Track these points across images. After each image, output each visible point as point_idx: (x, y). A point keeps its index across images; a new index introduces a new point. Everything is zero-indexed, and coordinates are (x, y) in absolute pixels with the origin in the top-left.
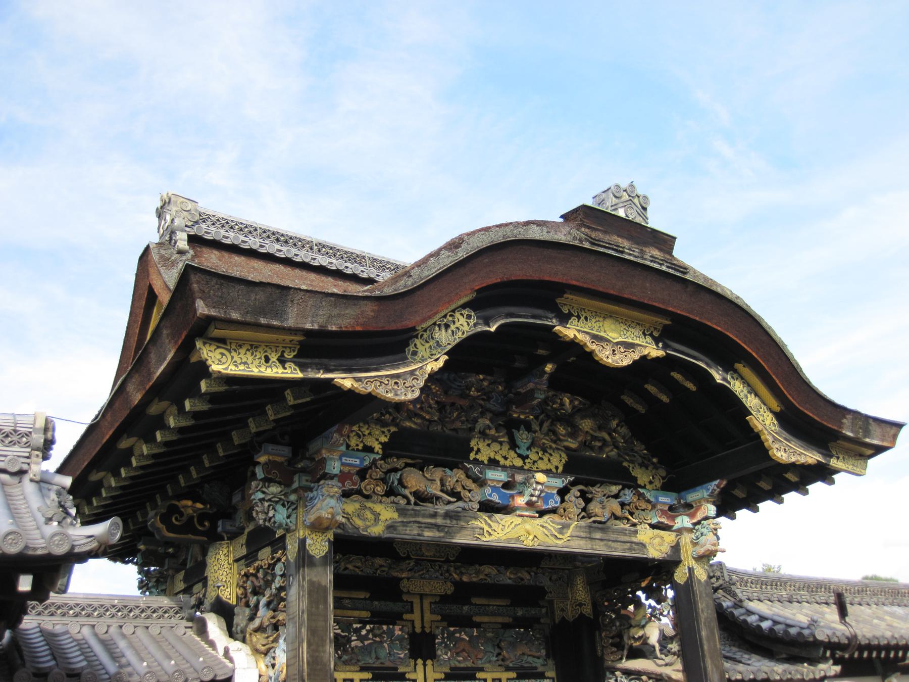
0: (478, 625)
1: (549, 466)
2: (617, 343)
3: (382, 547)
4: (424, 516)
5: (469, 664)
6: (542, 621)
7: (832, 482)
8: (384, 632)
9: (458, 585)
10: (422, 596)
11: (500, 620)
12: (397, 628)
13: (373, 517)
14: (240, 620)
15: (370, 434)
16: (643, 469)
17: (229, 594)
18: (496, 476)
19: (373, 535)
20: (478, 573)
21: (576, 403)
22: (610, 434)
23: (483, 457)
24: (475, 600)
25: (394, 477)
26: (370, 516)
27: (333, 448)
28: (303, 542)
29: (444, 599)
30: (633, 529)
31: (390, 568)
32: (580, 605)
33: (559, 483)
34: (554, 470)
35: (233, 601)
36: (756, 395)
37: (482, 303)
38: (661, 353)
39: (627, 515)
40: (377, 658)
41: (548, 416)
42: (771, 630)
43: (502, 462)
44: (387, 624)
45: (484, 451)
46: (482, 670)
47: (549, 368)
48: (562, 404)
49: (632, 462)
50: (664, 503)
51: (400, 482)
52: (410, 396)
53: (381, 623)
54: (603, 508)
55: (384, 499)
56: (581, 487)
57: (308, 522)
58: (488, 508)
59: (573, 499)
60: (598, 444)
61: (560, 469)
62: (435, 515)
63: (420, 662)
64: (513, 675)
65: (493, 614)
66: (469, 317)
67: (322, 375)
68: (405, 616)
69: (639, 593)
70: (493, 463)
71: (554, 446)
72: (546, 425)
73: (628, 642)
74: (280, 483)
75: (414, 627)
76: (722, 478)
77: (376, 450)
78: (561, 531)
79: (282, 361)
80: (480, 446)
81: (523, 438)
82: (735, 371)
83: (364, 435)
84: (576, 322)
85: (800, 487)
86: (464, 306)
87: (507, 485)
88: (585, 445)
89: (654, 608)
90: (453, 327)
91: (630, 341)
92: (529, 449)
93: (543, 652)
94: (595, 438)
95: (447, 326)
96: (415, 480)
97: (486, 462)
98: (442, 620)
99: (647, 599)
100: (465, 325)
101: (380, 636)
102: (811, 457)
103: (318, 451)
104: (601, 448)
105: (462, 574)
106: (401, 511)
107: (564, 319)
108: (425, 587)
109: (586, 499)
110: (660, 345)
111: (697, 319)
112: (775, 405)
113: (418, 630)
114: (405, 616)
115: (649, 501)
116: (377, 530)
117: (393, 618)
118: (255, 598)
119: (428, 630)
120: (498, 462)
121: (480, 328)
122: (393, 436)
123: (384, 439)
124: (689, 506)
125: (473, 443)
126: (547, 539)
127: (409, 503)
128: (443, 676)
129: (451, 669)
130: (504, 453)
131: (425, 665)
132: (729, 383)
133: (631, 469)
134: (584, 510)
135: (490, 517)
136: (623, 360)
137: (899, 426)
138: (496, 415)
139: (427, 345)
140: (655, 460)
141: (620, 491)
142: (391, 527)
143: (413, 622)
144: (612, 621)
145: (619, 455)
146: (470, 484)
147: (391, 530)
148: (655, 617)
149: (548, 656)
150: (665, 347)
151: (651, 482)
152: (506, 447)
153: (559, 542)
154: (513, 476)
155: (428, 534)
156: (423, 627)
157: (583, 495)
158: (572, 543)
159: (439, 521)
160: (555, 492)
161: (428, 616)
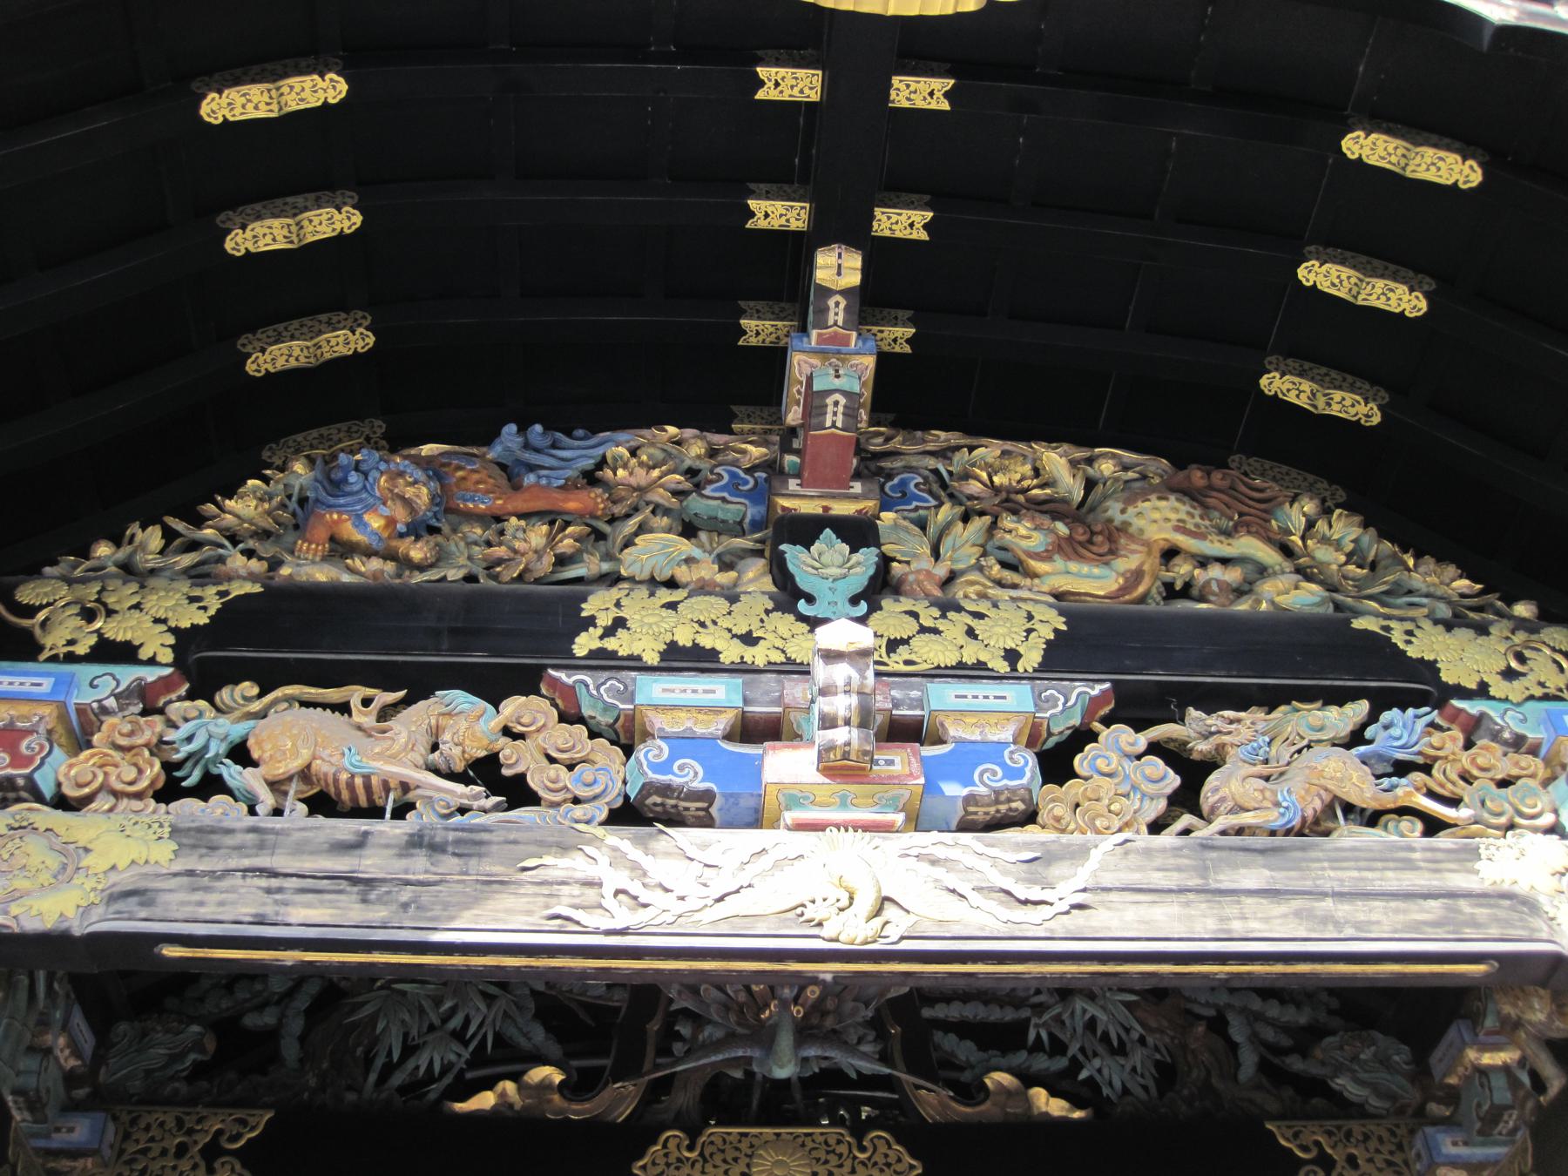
1: (971, 654)
4: (300, 849)
13: (54, 862)
15: (137, 606)
19: (31, 925)
22: (1287, 551)
23: (643, 642)
43: (731, 652)
45: (648, 628)
47: (838, 269)
51: (240, 754)
59: (1114, 761)
61: (1032, 658)
62: (359, 844)
70: (685, 659)
71: (1005, 594)
77: (144, 654)
83: (110, 613)
94: (1203, 562)
96: (299, 733)
97: (652, 658)
115: (1518, 743)
120: (713, 654)
125: (598, 605)
127: (252, 811)
133: (1397, 638)
135: (639, 842)
145: (1338, 607)
147: (131, 904)
151: (1509, 674)
155: (307, 915)
159: (370, 864)
160: (1007, 735)
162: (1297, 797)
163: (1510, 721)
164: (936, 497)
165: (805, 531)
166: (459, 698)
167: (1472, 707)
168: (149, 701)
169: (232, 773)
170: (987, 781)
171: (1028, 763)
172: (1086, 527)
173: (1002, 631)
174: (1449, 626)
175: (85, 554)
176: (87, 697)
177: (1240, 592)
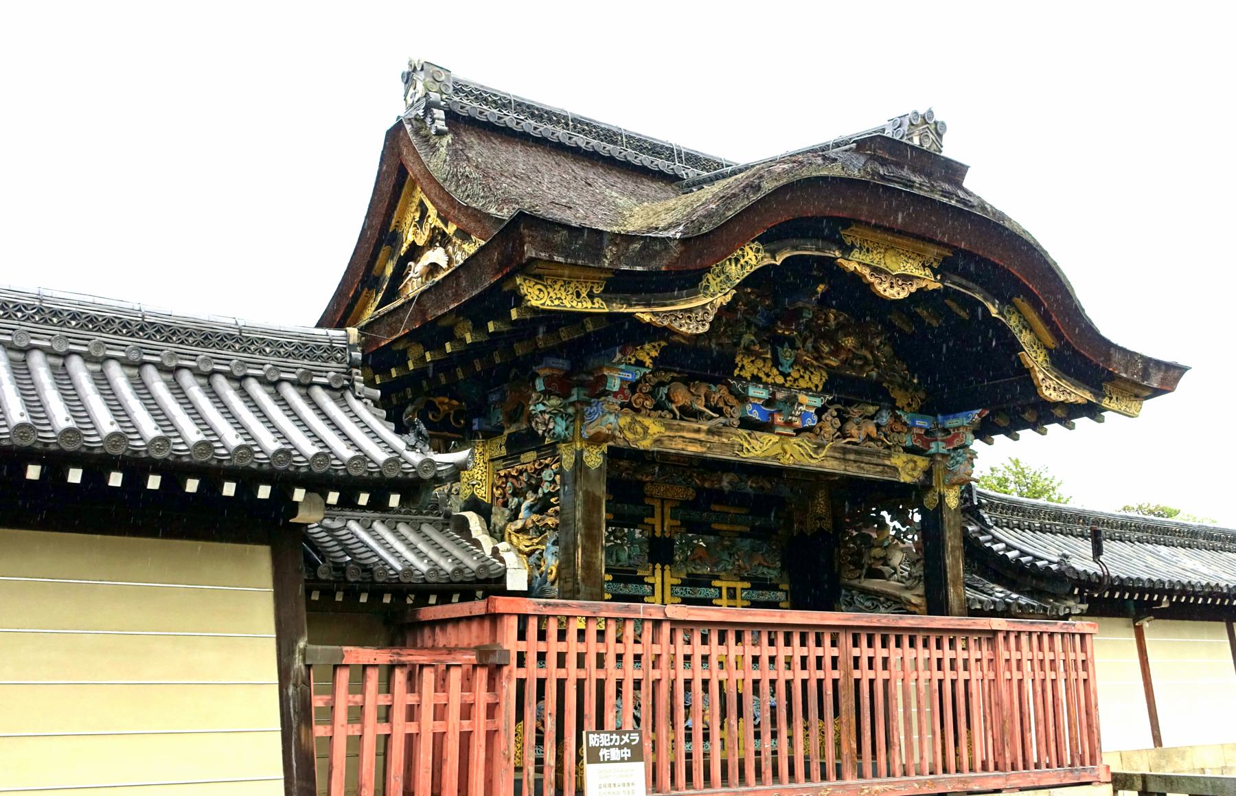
1: (810, 385)
2: (896, 276)
3: (640, 457)
4: (689, 431)
6: (780, 532)
7: (1101, 420)
8: (625, 535)
9: (699, 490)
10: (662, 500)
12: (637, 531)
14: (498, 519)
17: (483, 493)
18: (758, 393)
21: (841, 318)
22: (872, 353)
23: (747, 374)
25: (664, 391)
26: (639, 430)
27: (613, 367)
28: (579, 455)
29: (685, 504)
30: (886, 452)
31: (635, 471)
32: (820, 519)
33: (818, 402)
35: (487, 500)
36: (1031, 330)
37: (770, 240)
38: (938, 285)
39: (882, 437)
40: (618, 560)
41: (811, 331)
42: (1018, 560)
43: (764, 379)
44: (629, 527)
45: (749, 368)
46: (717, 578)
48: (827, 320)
49: (891, 382)
50: (921, 428)
52: (701, 330)
54: (859, 429)
55: (653, 413)
56: (839, 406)
57: (586, 435)
58: (747, 423)
59: (829, 418)
60: (860, 363)
62: (698, 431)
63: (658, 566)
64: (747, 585)
65: (732, 523)
66: (758, 251)
67: (625, 310)
68: (647, 520)
69: (884, 513)
70: (756, 379)
72: (809, 344)
73: (866, 560)
74: (558, 396)
75: (654, 531)
76: (984, 408)
78: (816, 450)
79: (591, 296)
80: (745, 362)
81: (787, 355)
82: (1013, 305)
84: (857, 255)
85: (1066, 421)
87: (769, 402)
89: (898, 531)
90: (742, 261)
92: (791, 366)
93: (779, 564)
95: (737, 260)
96: (682, 396)
98: (682, 526)
99: (892, 520)
100: (753, 258)
101: (621, 538)
102: (1081, 395)
103: (600, 368)
104: (861, 367)
105: (704, 480)
106: (669, 427)
107: (847, 250)
108: (665, 493)
112: (1050, 341)
114: (647, 520)
115: (905, 424)
116: (645, 444)
117: (635, 521)
118: (516, 500)
119: (667, 535)
120: (760, 379)
121: (768, 261)
122: (663, 350)
123: (654, 354)
124: (946, 431)
125: (738, 359)
129: (688, 575)
130: (767, 370)
131: (663, 570)
134: (839, 429)
136: (898, 293)
137: (1182, 370)
138: (761, 330)
139: (718, 280)
141: (877, 412)
142: (658, 441)
143: (653, 526)
144: (853, 539)
146: (732, 400)
148: (899, 539)
149: (782, 569)
150: (941, 281)
151: (909, 405)
152: (769, 364)
153: (813, 461)
154: (773, 394)
156: (663, 531)
158: (826, 463)
159: (702, 436)
163: (905, 418)
167: (899, 413)
173: (816, 379)
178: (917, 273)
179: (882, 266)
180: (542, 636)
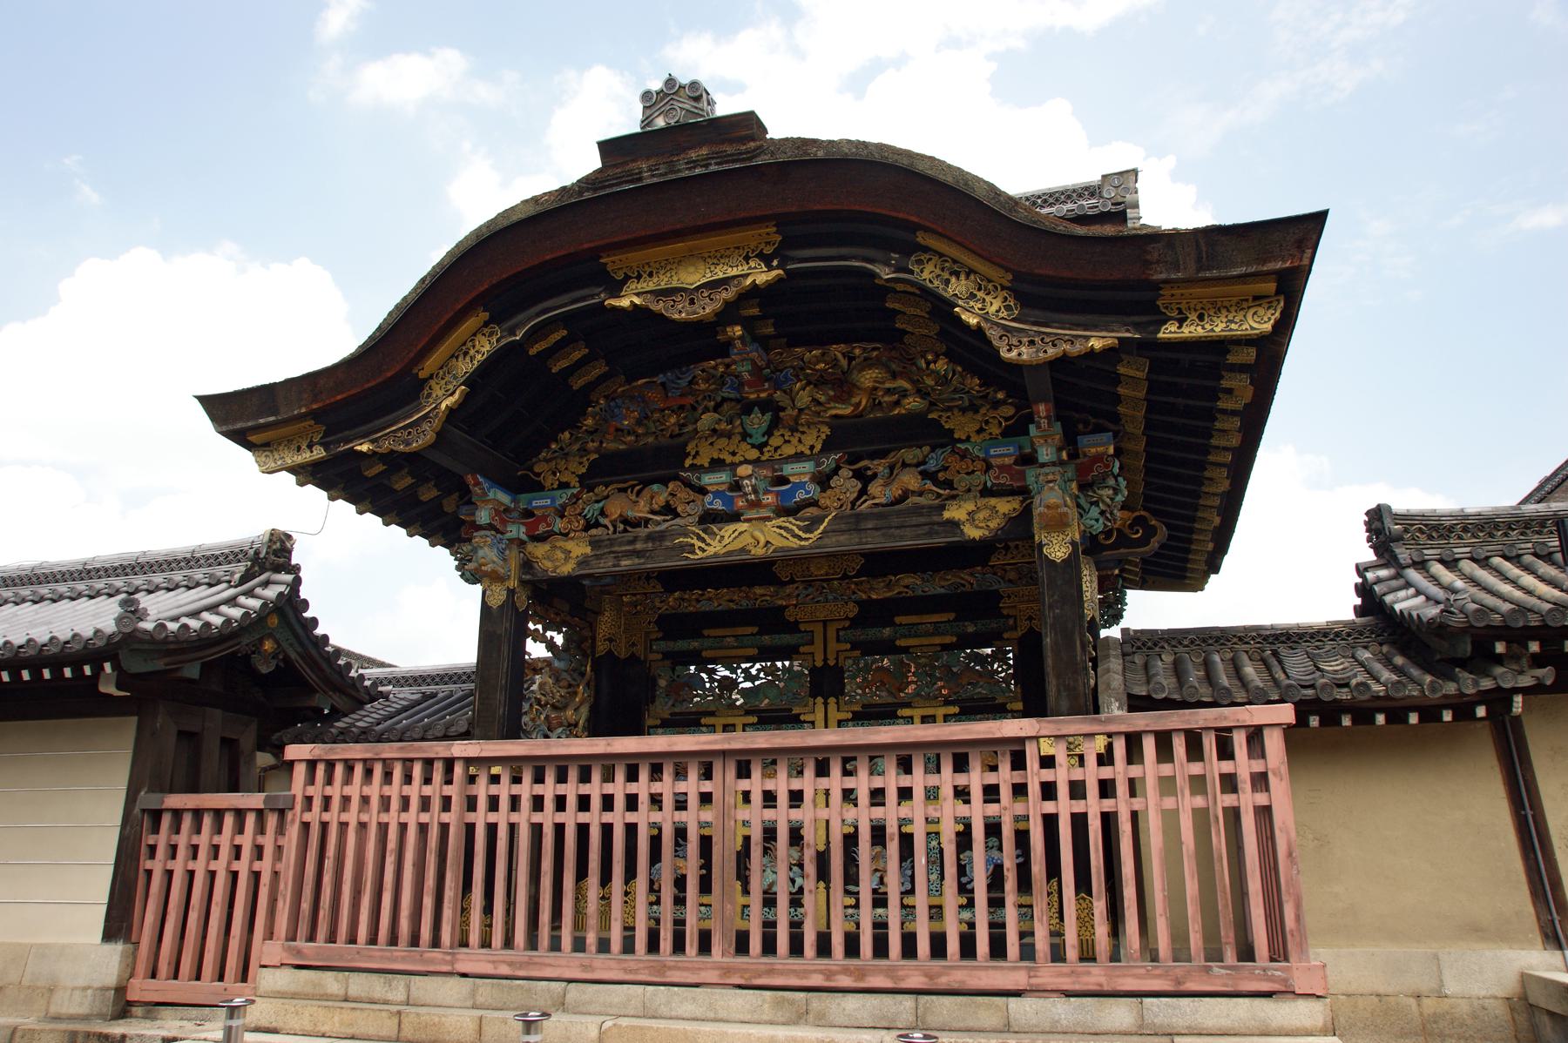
0: (906, 650)
1: (801, 448)
4: (621, 544)
5: (891, 700)
10: (825, 623)
11: (937, 640)
16: (970, 414)
20: (889, 586)
24: (898, 620)
26: (560, 555)
29: (855, 623)
34: (808, 452)
43: (729, 459)
51: (603, 513)
53: (773, 660)
58: (710, 519)
61: (818, 447)
62: (633, 542)
65: (927, 634)
66: (491, 334)
68: (802, 649)
70: (717, 465)
86: (486, 324)
88: (876, 405)
90: (472, 352)
91: (721, 275)
94: (888, 391)
95: (466, 354)
96: (618, 507)
100: (485, 347)
107: (616, 289)
109: (864, 478)
110: (775, 263)
111: (794, 209)
113: (819, 664)
114: (802, 649)
116: (567, 569)
119: (832, 663)
122: (593, 464)
125: (690, 448)
126: (785, 543)
128: (850, 716)
131: (826, 704)
132: (912, 272)
140: (1000, 396)
142: (584, 562)
146: (684, 494)
152: (737, 438)
156: (825, 660)
157: (858, 475)
159: (639, 546)
161: (833, 646)
162: (895, 491)
164: (797, 376)
165: (747, 409)
166: (655, 487)
168: (577, 497)
169: (603, 521)
170: (800, 496)
171: (812, 487)
172: (842, 386)
174: (963, 410)
175: (548, 447)
176: (559, 502)
177: (897, 403)
178: (735, 272)
179: (675, 284)
180: (408, 779)
